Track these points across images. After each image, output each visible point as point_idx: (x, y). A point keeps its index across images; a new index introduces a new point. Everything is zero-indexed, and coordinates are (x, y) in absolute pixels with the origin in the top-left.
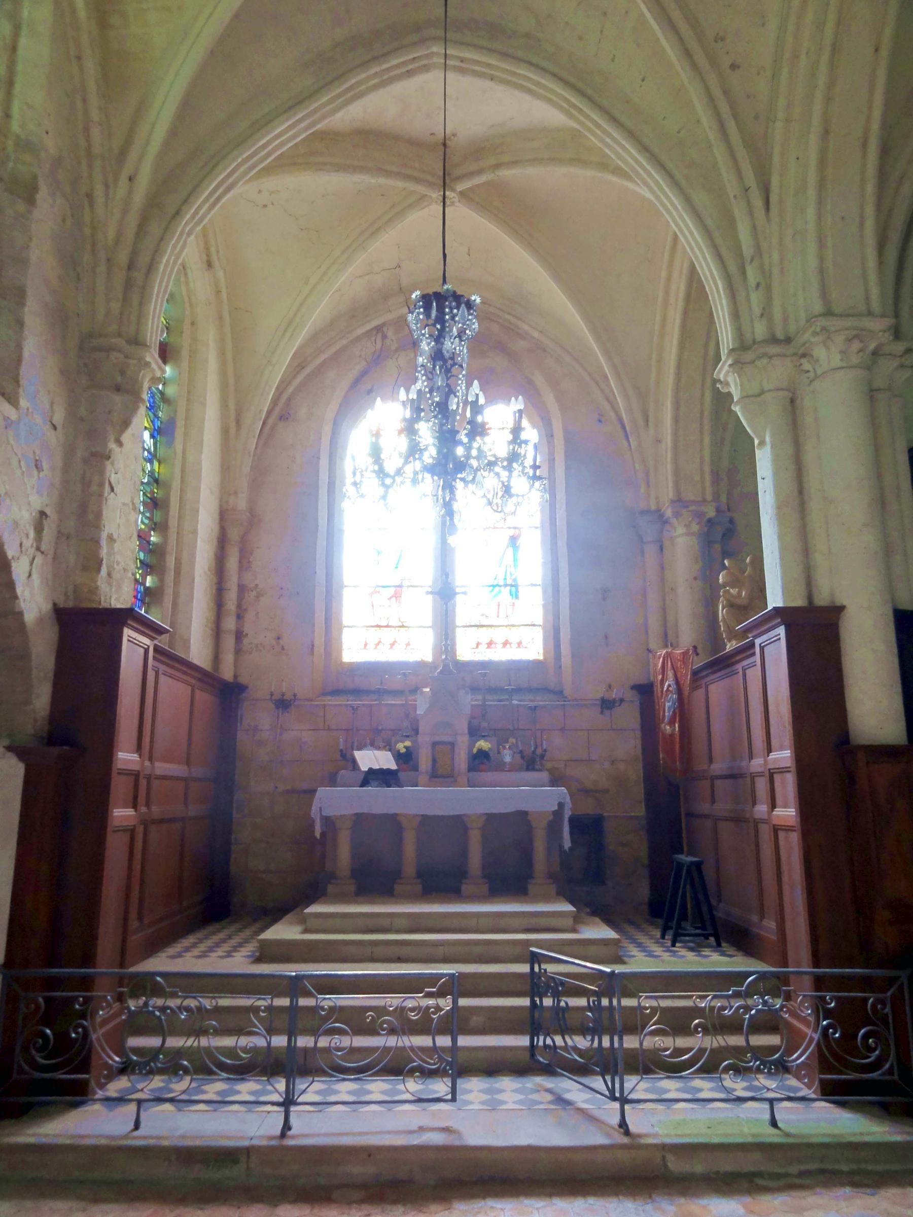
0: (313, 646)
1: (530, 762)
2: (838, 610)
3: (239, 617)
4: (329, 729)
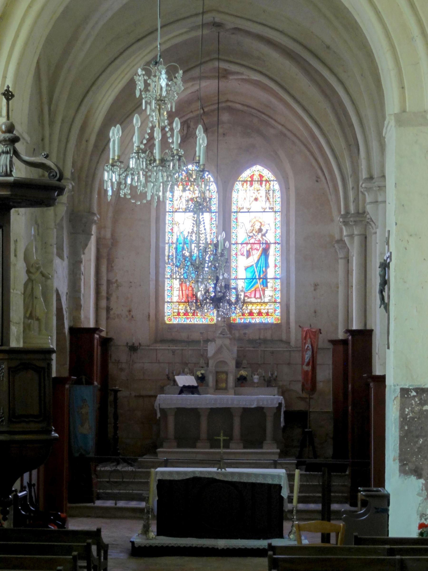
0: (149, 315)
1: (269, 382)
2: (371, 331)
3: (108, 299)
4: (159, 363)
